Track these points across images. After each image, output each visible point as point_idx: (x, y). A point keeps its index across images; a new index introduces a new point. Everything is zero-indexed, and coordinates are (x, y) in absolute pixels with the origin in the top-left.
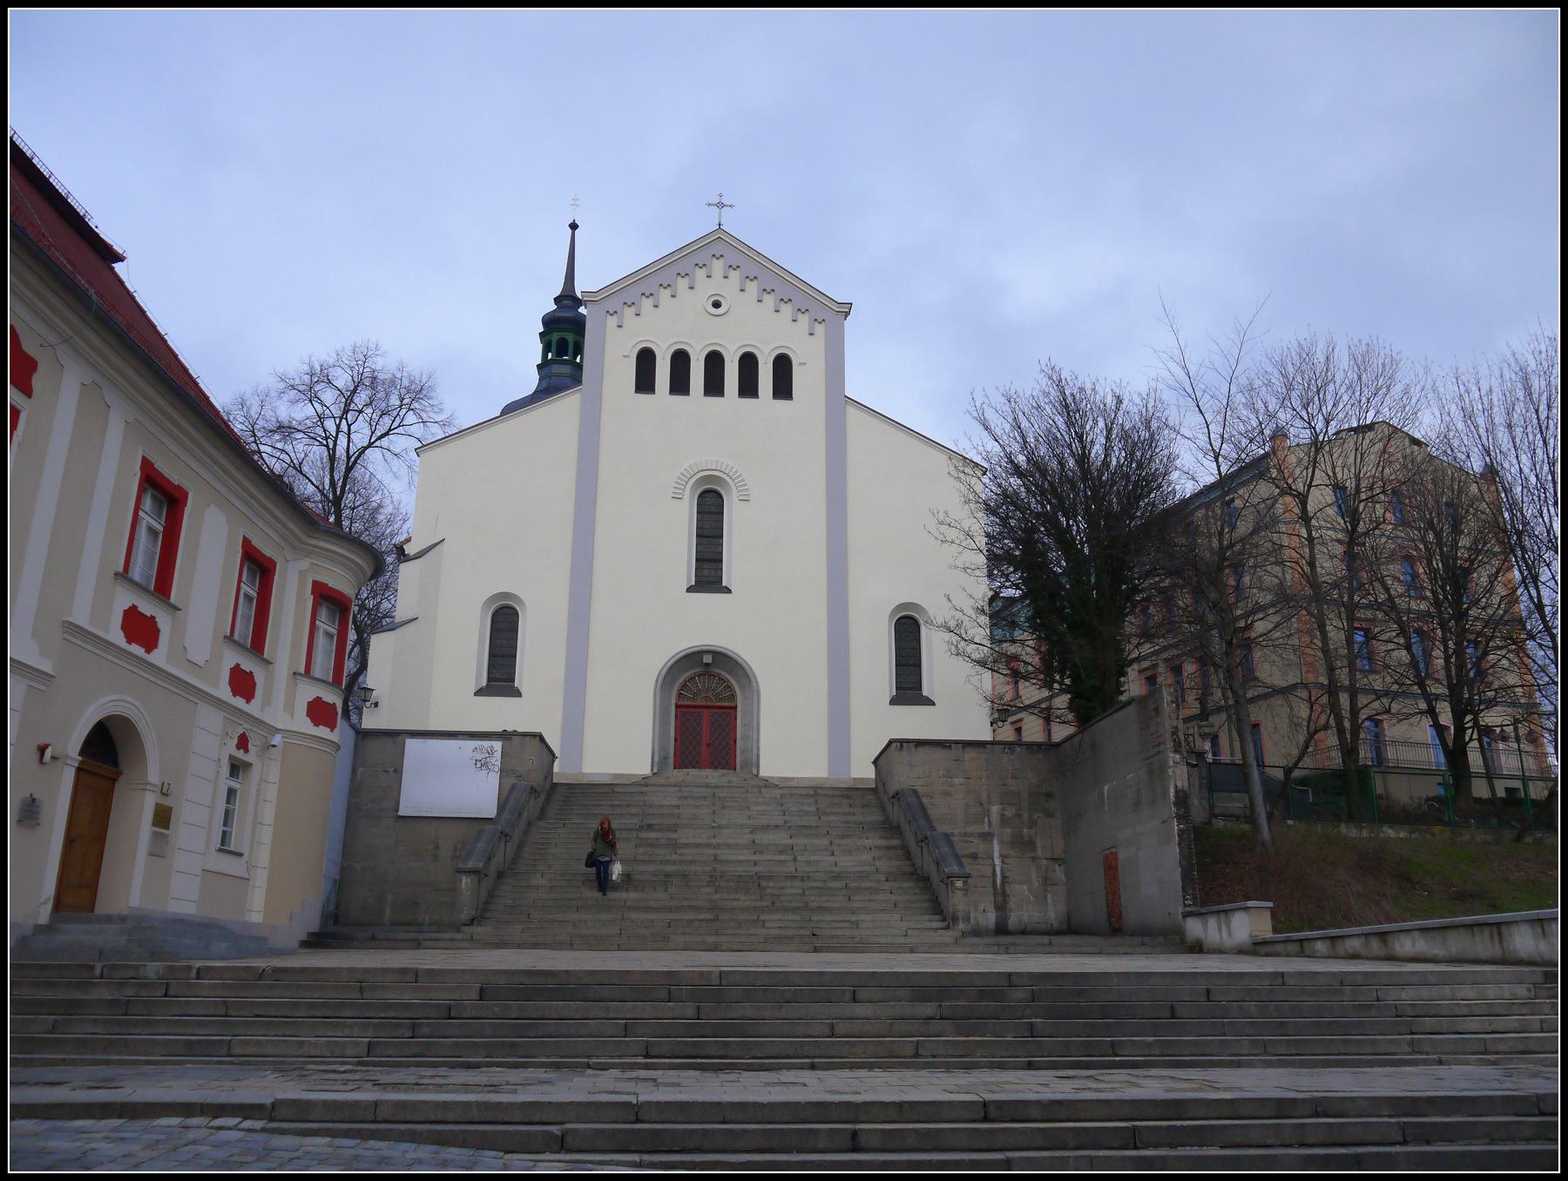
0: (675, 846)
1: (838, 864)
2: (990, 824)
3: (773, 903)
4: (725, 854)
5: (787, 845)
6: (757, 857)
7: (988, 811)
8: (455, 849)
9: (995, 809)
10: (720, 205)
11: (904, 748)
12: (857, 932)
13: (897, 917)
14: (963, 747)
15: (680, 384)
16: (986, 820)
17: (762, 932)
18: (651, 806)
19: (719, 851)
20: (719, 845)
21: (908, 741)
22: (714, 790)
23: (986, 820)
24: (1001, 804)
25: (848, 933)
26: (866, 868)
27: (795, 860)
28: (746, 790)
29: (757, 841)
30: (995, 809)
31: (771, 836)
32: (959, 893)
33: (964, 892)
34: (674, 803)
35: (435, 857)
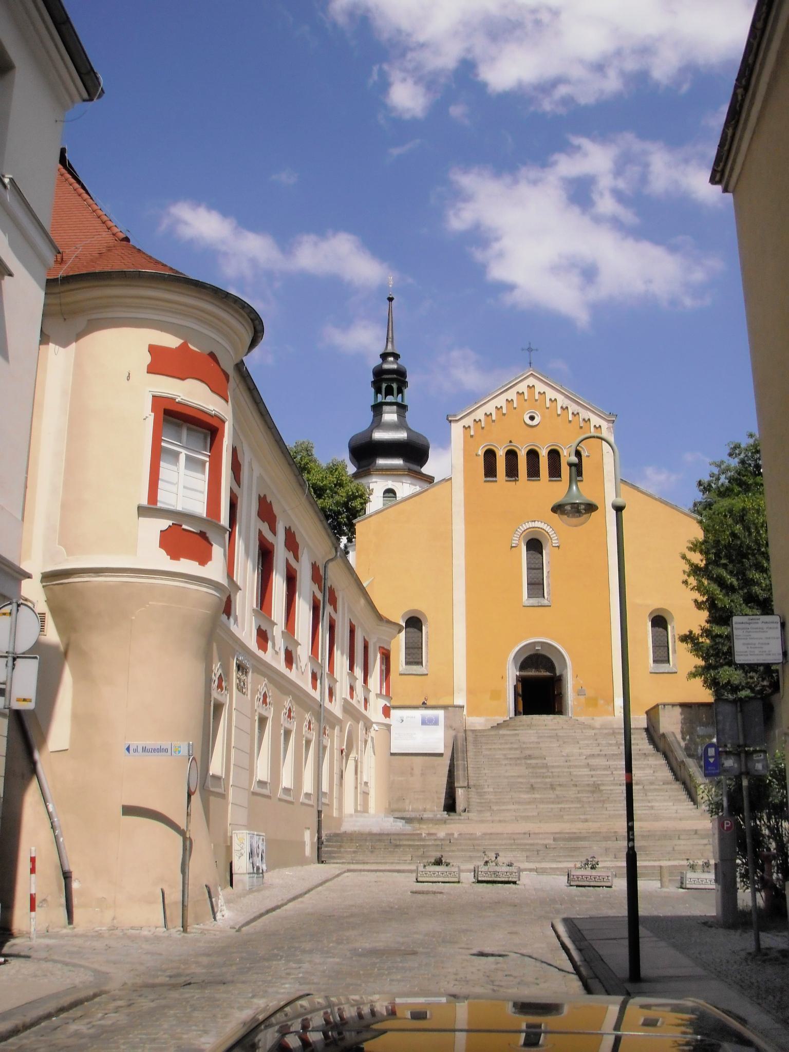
0: (546, 766)
3: (608, 798)
4: (575, 772)
5: (606, 765)
6: (593, 773)
8: (422, 770)
10: (530, 350)
12: (653, 812)
13: (671, 804)
17: (606, 812)
18: (524, 743)
19: (572, 770)
20: (570, 766)
22: (555, 732)
25: (647, 812)
26: (651, 778)
27: (612, 773)
28: (574, 731)
29: (590, 763)
31: (597, 760)
34: (536, 740)
35: (412, 775)
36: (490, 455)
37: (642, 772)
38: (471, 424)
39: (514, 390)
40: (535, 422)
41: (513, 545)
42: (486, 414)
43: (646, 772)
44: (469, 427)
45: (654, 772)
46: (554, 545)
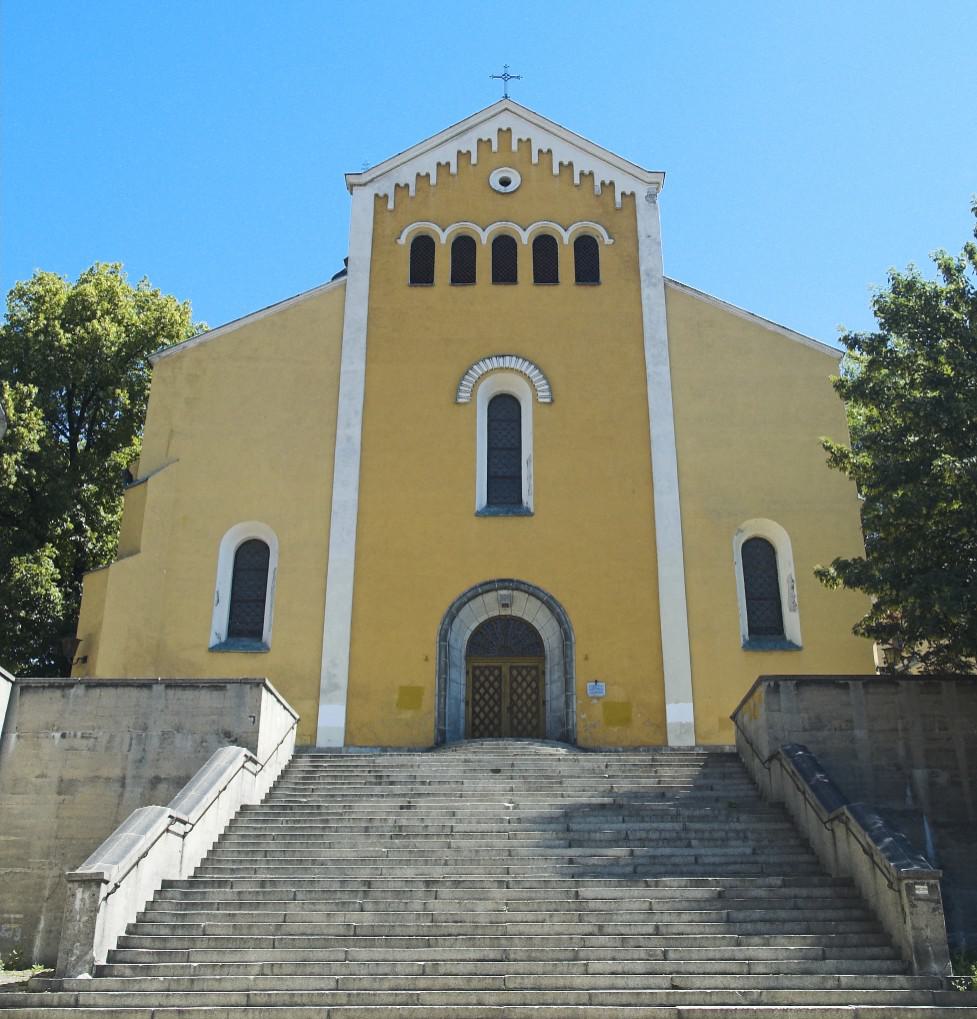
1: (700, 861)
2: (915, 797)
7: (911, 777)
9: (920, 775)
10: (506, 77)
11: (781, 689)
14: (865, 685)
15: (463, 273)
16: (909, 793)
21: (787, 678)
23: (909, 793)
24: (928, 767)
30: (920, 775)
32: (923, 907)
33: (933, 905)
36: (422, 248)
37: (718, 851)
38: (391, 193)
39: (474, 136)
40: (510, 188)
41: (460, 400)
42: (418, 175)
43: (730, 851)
44: (386, 196)
45: (754, 853)
46: (541, 400)
